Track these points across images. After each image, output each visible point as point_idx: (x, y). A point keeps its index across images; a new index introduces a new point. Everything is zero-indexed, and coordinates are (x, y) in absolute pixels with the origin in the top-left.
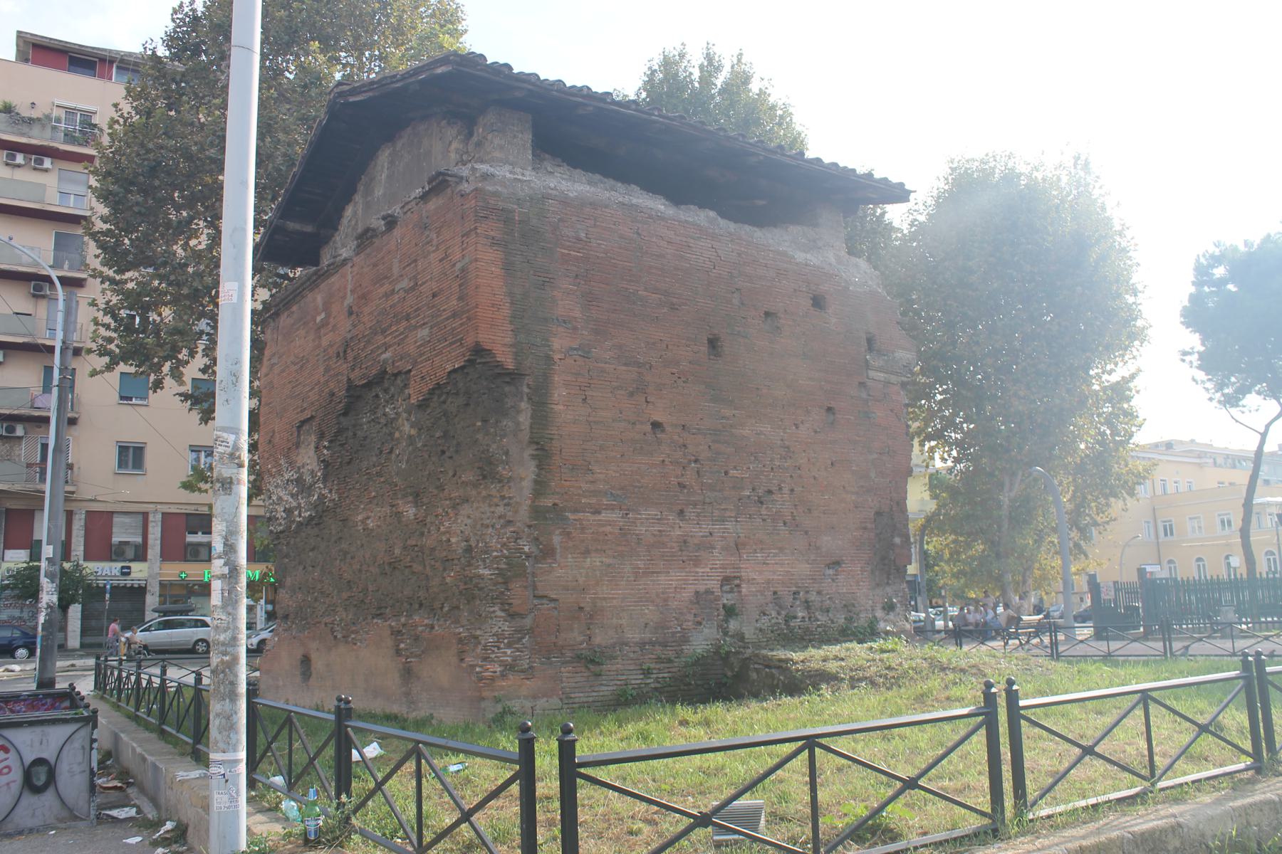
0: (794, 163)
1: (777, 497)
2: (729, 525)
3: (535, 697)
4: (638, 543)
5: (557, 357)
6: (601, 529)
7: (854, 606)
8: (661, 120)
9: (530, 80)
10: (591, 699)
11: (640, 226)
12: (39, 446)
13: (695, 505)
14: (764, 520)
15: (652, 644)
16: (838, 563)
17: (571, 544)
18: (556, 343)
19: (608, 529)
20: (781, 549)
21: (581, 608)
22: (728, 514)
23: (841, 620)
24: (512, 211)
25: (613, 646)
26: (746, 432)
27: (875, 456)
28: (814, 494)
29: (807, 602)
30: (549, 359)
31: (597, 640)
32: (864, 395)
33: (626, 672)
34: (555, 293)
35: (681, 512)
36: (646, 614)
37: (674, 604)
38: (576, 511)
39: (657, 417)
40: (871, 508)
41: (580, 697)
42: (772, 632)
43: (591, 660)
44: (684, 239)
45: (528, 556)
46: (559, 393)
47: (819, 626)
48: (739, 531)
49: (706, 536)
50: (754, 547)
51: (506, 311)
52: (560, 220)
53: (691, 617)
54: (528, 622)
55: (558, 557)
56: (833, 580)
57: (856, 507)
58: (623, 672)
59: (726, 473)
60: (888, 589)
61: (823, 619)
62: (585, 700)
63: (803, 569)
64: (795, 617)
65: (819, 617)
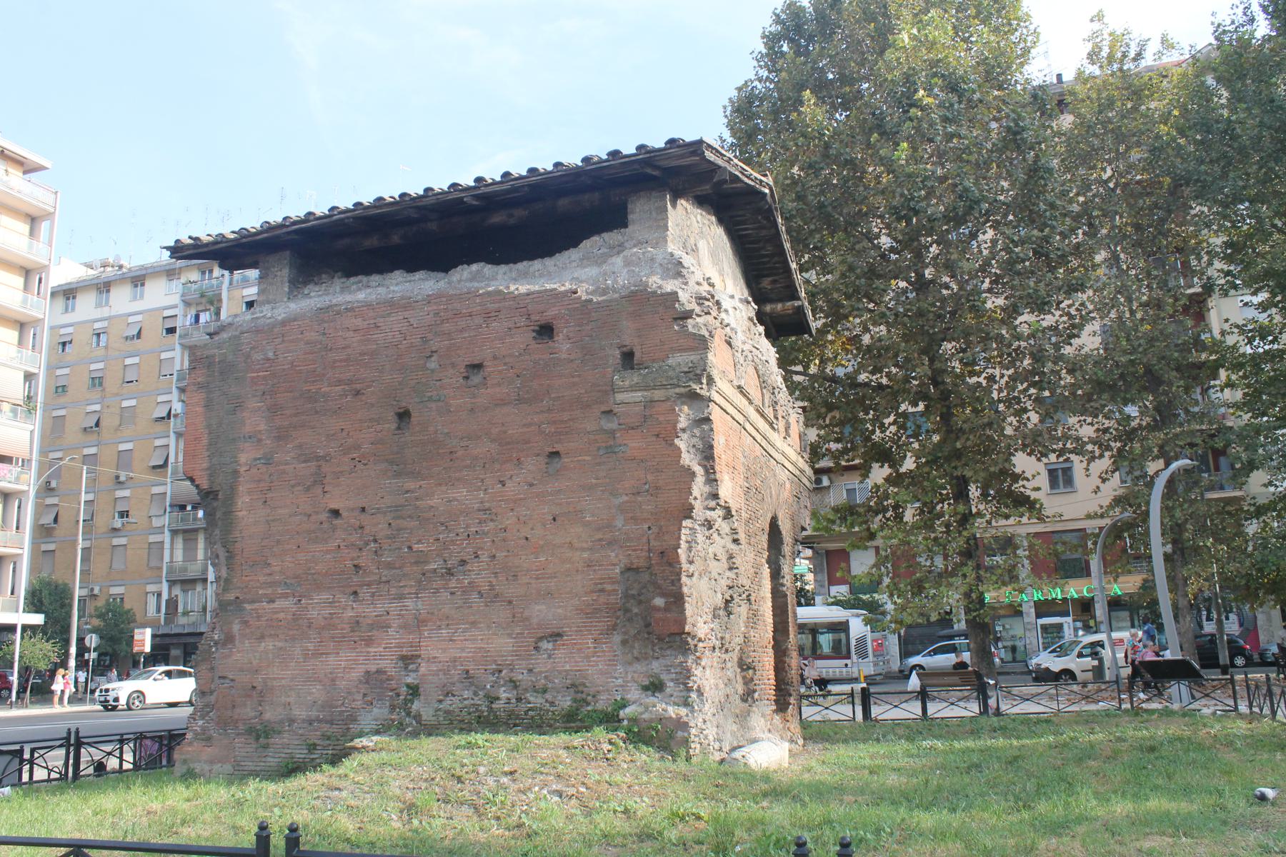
0: (505, 187)
1: (474, 566)
2: (409, 603)
3: (212, 762)
4: (309, 627)
5: (242, 469)
6: (275, 616)
7: (584, 685)
8: (343, 216)
9: (268, 228)
10: (258, 768)
11: (326, 325)
12: (845, 492)
13: (369, 585)
14: (452, 593)
15: (320, 721)
16: (559, 635)
17: (248, 631)
18: (243, 458)
19: (281, 616)
20: (474, 623)
21: (254, 687)
22: (406, 591)
23: (565, 702)
24: (213, 356)
25: (281, 722)
26: (435, 501)
27: (625, 498)
28: (523, 557)
29: (511, 681)
30: (236, 473)
31: (267, 716)
32: (612, 425)
33: (291, 747)
34: (244, 414)
35: (355, 593)
36: (313, 693)
37: (342, 684)
38: (253, 602)
39: (334, 506)
40: (614, 565)
41: (250, 765)
42: (470, 714)
43: (261, 733)
44: (372, 322)
45: (216, 643)
46: (243, 500)
47: (530, 709)
48: (420, 607)
49: (380, 616)
50: (438, 623)
51: (205, 441)
52: (251, 348)
53: (359, 697)
54: (212, 698)
55: (237, 642)
56: (550, 657)
57: (588, 566)
58: (287, 745)
59: (410, 548)
60: (656, 666)
61: (536, 700)
62: (253, 768)
63: (502, 644)
64: (498, 699)
65: (532, 699)
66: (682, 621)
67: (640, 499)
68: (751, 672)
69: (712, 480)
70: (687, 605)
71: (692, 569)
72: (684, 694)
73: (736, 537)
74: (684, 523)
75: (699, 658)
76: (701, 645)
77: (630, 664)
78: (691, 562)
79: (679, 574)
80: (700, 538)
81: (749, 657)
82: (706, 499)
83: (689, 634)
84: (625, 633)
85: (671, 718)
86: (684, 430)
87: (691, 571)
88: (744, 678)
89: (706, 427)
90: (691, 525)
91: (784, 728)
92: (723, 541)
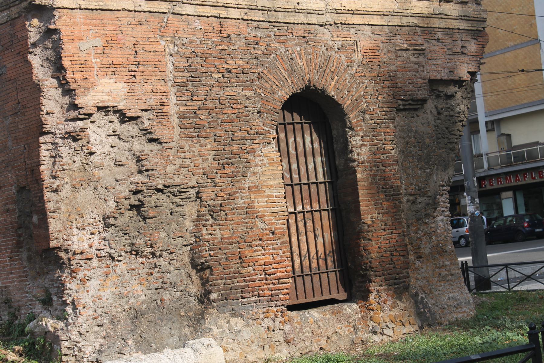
40: (12, 185)
66: (47, 238)
67: (17, 119)
68: (207, 272)
69: (68, 92)
70: (51, 221)
71: (57, 183)
72: (62, 307)
73: (150, 136)
74: (42, 139)
75: (72, 271)
76: (78, 257)
77: (35, 278)
78: (55, 177)
79: (42, 191)
80: (64, 151)
81: (201, 257)
82: (68, 110)
83: (59, 248)
84: (29, 250)
85: (50, 331)
86: (34, 45)
87: (55, 186)
88: (201, 278)
89: (55, 37)
90: (51, 140)
91: (364, 318)
92: (128, 145)
